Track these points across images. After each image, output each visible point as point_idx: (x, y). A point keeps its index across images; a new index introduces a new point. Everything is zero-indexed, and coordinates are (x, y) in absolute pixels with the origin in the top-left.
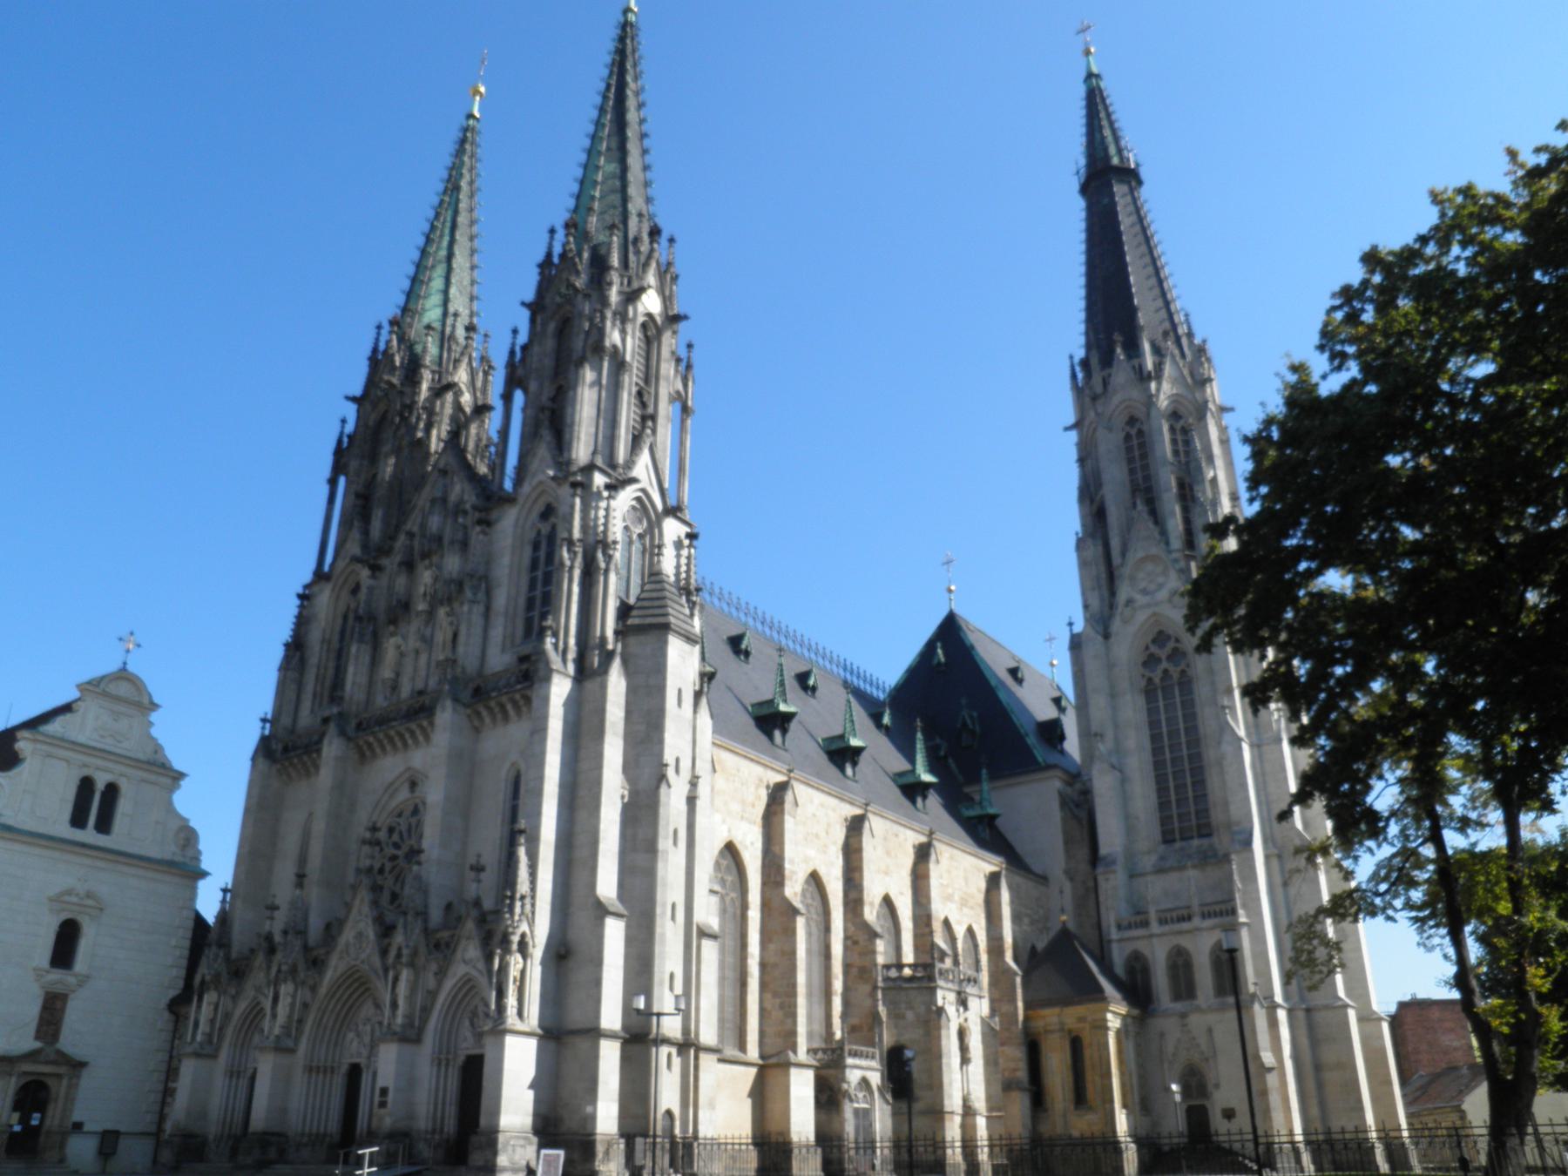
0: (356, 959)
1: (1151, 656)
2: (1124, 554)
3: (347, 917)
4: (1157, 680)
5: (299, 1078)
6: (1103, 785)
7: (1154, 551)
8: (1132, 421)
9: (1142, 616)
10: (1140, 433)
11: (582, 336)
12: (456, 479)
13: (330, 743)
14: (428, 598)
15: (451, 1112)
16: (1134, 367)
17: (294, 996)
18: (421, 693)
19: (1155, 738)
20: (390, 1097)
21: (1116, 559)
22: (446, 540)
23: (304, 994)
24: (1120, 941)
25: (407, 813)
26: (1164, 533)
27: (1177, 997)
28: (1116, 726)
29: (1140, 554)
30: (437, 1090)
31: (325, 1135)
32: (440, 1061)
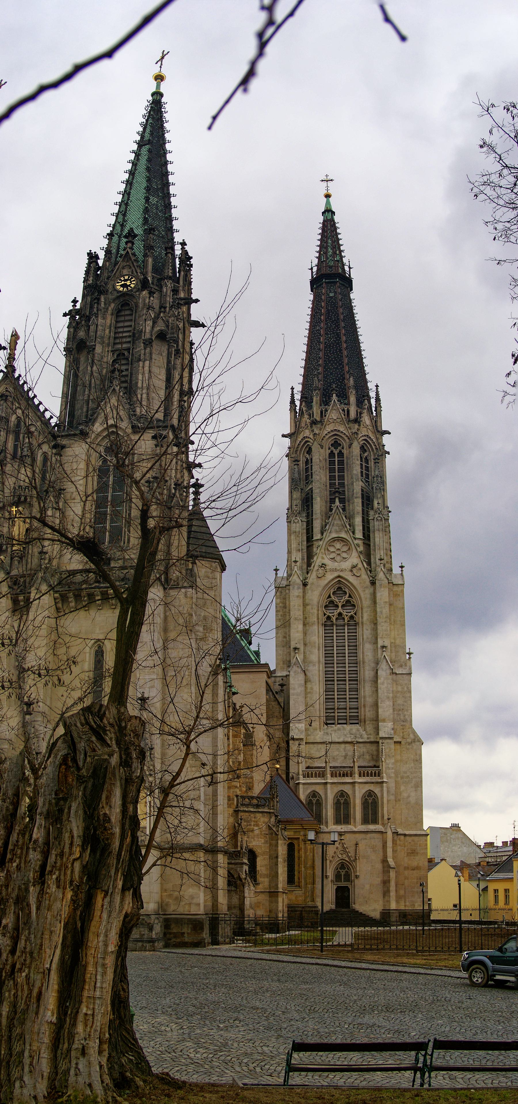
1: (332, 602)
2: (322, 534)
4: (334, 619)
6: (296, 682)
7: (343, 535)
8: (336, 444)
9: (330, 576)
10: (341, 454)
11: (150, 323)
16: (343, 410)
19: (328, 655)
21: (317, 536)
24: (304, 784)
26: (352, 525)
27: (338, 821)
28: (305, 645)
29: (334, 535)
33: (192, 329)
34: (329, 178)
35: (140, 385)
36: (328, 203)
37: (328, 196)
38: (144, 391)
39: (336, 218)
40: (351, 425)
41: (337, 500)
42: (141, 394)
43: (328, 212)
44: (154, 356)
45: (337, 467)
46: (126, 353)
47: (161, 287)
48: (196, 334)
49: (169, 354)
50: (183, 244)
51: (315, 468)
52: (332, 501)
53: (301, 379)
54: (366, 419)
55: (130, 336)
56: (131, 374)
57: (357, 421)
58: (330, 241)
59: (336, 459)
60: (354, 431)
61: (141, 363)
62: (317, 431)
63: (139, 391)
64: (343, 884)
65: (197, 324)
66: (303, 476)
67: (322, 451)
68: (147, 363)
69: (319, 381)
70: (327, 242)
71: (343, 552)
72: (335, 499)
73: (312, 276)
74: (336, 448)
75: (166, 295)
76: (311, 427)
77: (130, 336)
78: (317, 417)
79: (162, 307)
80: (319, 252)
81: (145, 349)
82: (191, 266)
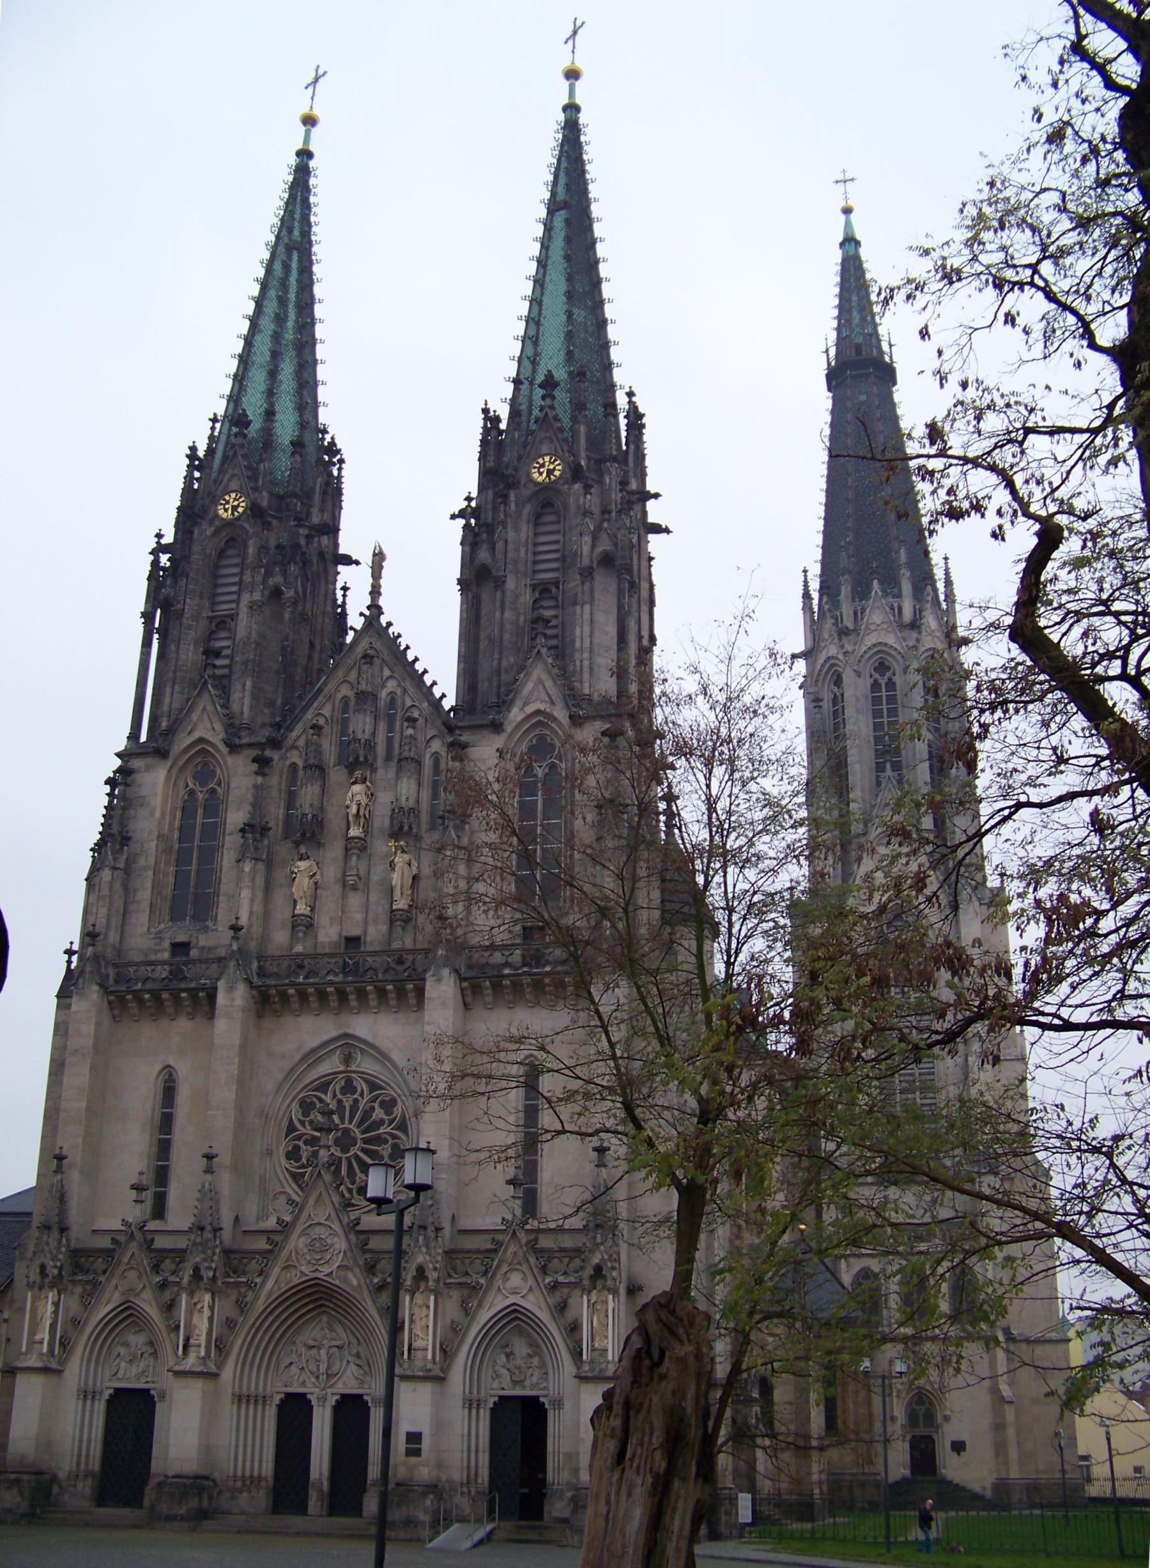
3: (297, 1218)
5: (228, 1409)
8: (882, 667)
10: (891, 684)
11: (587, 539)
12: (387, 673)
13: (231, 989)
14: (362, 820)
15: (484, 1459)
16: (892, 608)
17: (212, 1308)
18: (353, 941)
20: (426, 1444)
22: (381, 750)
23: (226, 1307)
25: (337, 1086)
30: (469, 1435)
31: (260, 1478)
32: (472, 1404)
33: (651, 537)
34: (848, 176)
35: (578, 645)
36: (848, 225)
37: (847, 211)
38: (586, 655)
39: (864, 253)
40: (906, 633)
41: (888, 766)
42: (582, 659)
43: (850, 242)
44: (596, 595)
45: (885, 707)
46: (554, 590)
47: (601, 474)
48: (655, 543)
49: (620, 592)
50: (630, 394)
51: (849, 712)
52: (880, 768)
53: (818, 554)
54: (930, 621)
55: (556, 560)
56: (563, 624)
57: (915, 625)
58: (855, 298)
59: (884, 693)
60: (911, 643)
61: (578, 608)
62: (848, 647)
63: (577, 656)
64: (922, 1430)
65: (657, 529)
66: (829, 724)
67: (860, 681)
68: (587, 607)
69: (849, 557)
70: (849, 300)
71: (899, 855)
72: (884, 763)
73: (829, 364)
74: (882, 675)
75: (610, 489)
76: (840, 639)
77: (556, 560)
78: (849, 623)
79: (605, 511)
80: (839, 318)
81: (583, 583)
82: (643, 426)
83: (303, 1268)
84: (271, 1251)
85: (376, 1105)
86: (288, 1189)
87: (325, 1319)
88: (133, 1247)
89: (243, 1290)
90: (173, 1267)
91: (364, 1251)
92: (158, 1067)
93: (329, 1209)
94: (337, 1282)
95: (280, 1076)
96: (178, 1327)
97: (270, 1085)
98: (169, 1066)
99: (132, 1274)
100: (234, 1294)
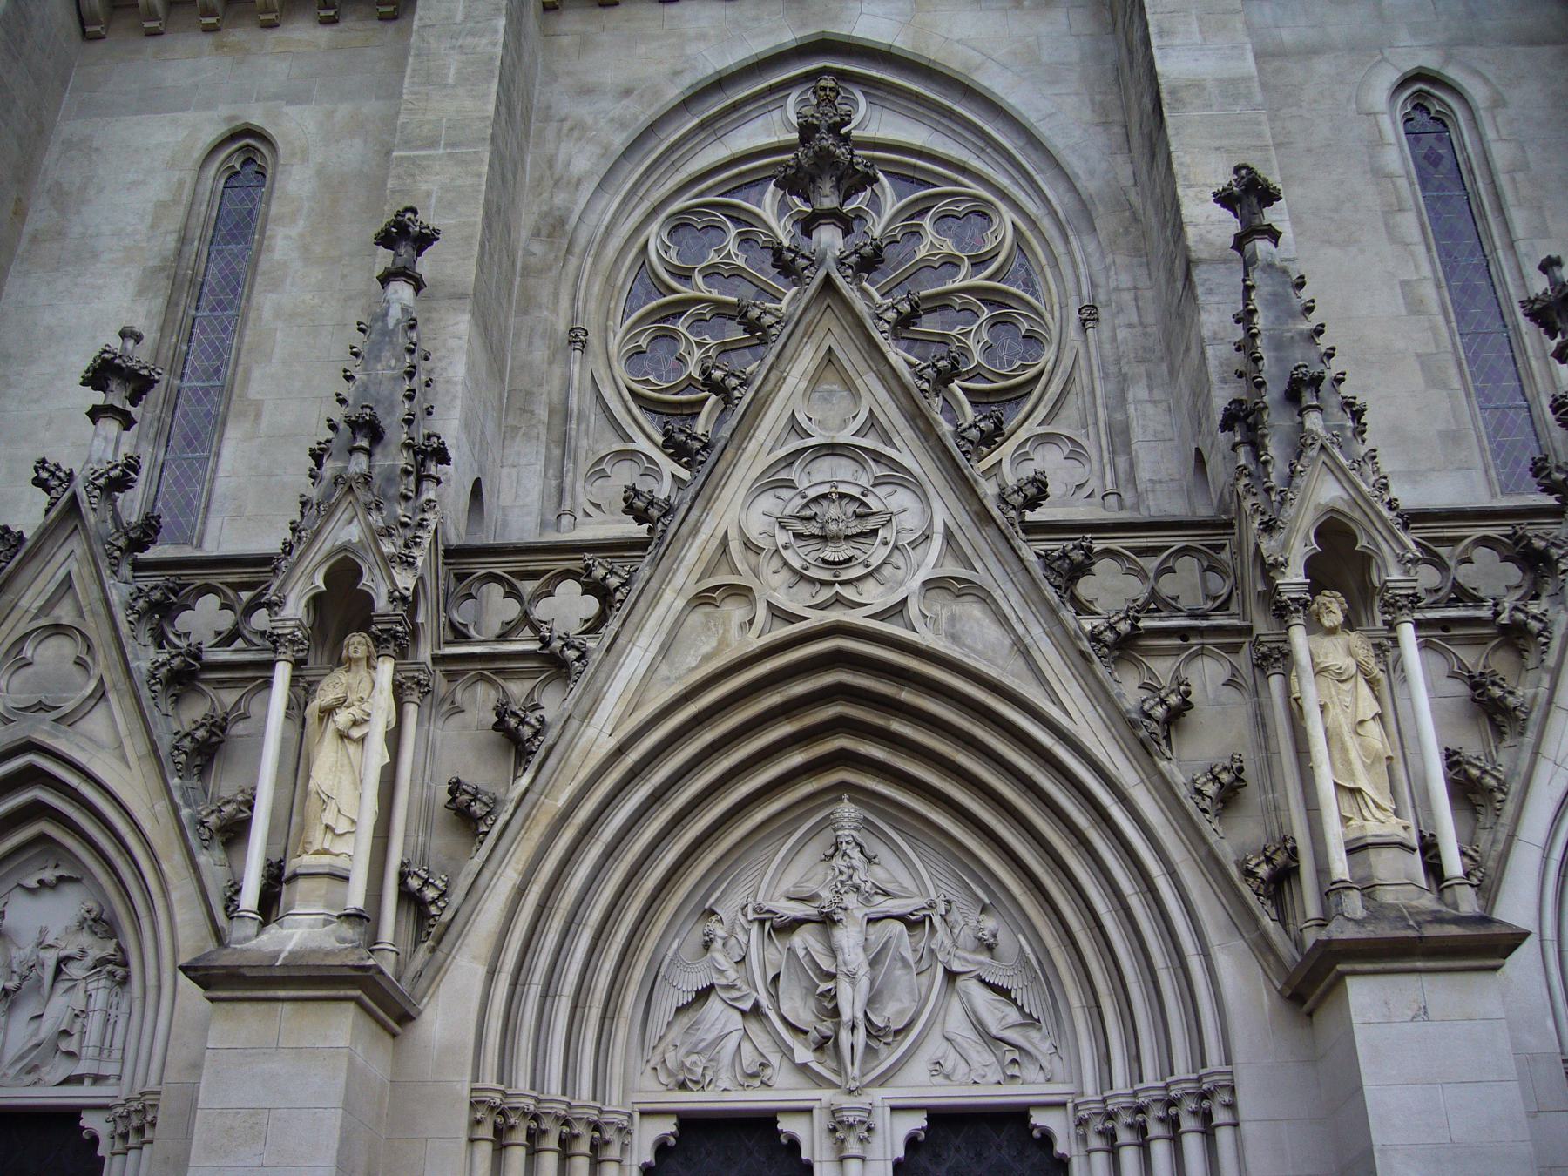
0: (838, 600)
17: (394, 738)
83: (783, 600)
84: (640, 545)
85: (927, 222)
86: (642, 444)
87: (847, 810)
88: (69, 557)
89: (518, 689)
90: (227, 620)
91: (1031, 529)
92: (212, 133)
93: (875, 395)
94: (926, 637)
95: (619, 141)
96: (234, 833)
97: (583, 161)
98: (249, 132)
99: (53, 654)
100: (480, 702)
